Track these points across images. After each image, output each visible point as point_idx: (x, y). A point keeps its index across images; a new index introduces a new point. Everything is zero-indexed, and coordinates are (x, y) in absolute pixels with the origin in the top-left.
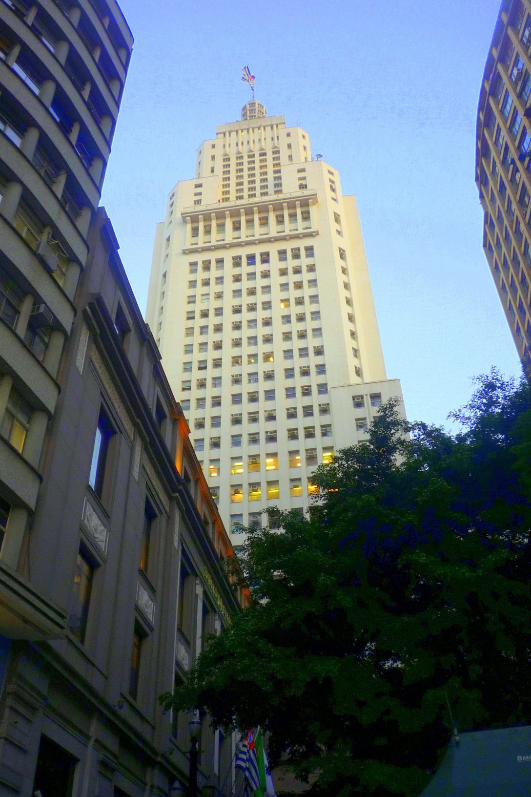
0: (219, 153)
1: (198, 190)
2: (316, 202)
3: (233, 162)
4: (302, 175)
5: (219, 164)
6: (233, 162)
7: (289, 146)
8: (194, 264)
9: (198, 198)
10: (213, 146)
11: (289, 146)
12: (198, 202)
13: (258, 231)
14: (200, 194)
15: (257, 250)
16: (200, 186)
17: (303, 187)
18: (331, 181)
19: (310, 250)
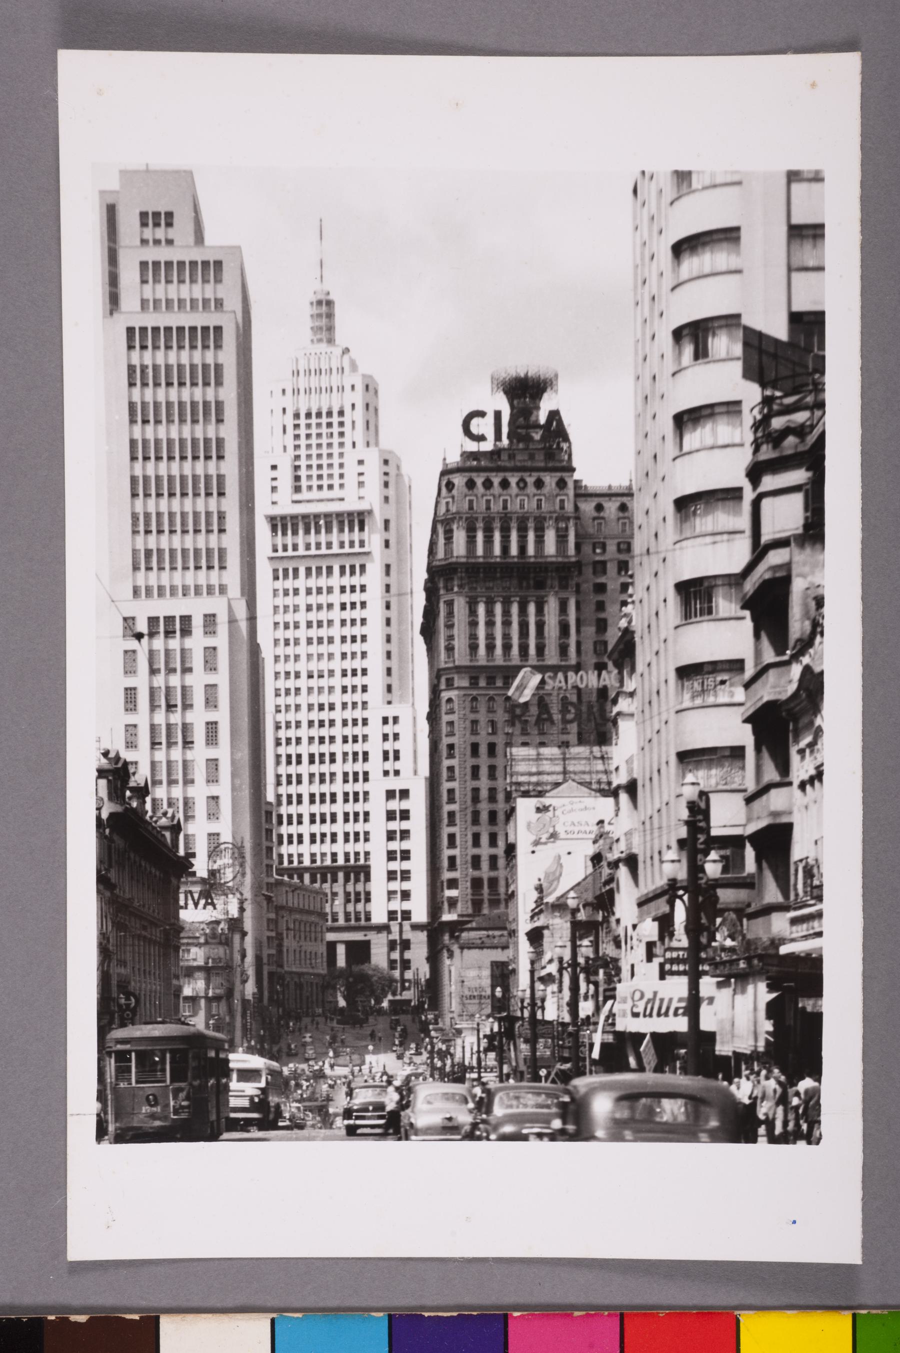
0: (288, 402)
1: (274, 474)
2: (370, 512)
3: (303, 421)
4: (361, 469)
5: (289, 421)
6: (303, 421)
7: (353, 405)
8: (275, 571)
9: (275, 483)
10: (284, 391)
11: (353, 405)
13: (323, 538)
14: (274, 479)
16: (274, 467)
17: (361, 484)
18: (386, 474)
19: (363, 568)
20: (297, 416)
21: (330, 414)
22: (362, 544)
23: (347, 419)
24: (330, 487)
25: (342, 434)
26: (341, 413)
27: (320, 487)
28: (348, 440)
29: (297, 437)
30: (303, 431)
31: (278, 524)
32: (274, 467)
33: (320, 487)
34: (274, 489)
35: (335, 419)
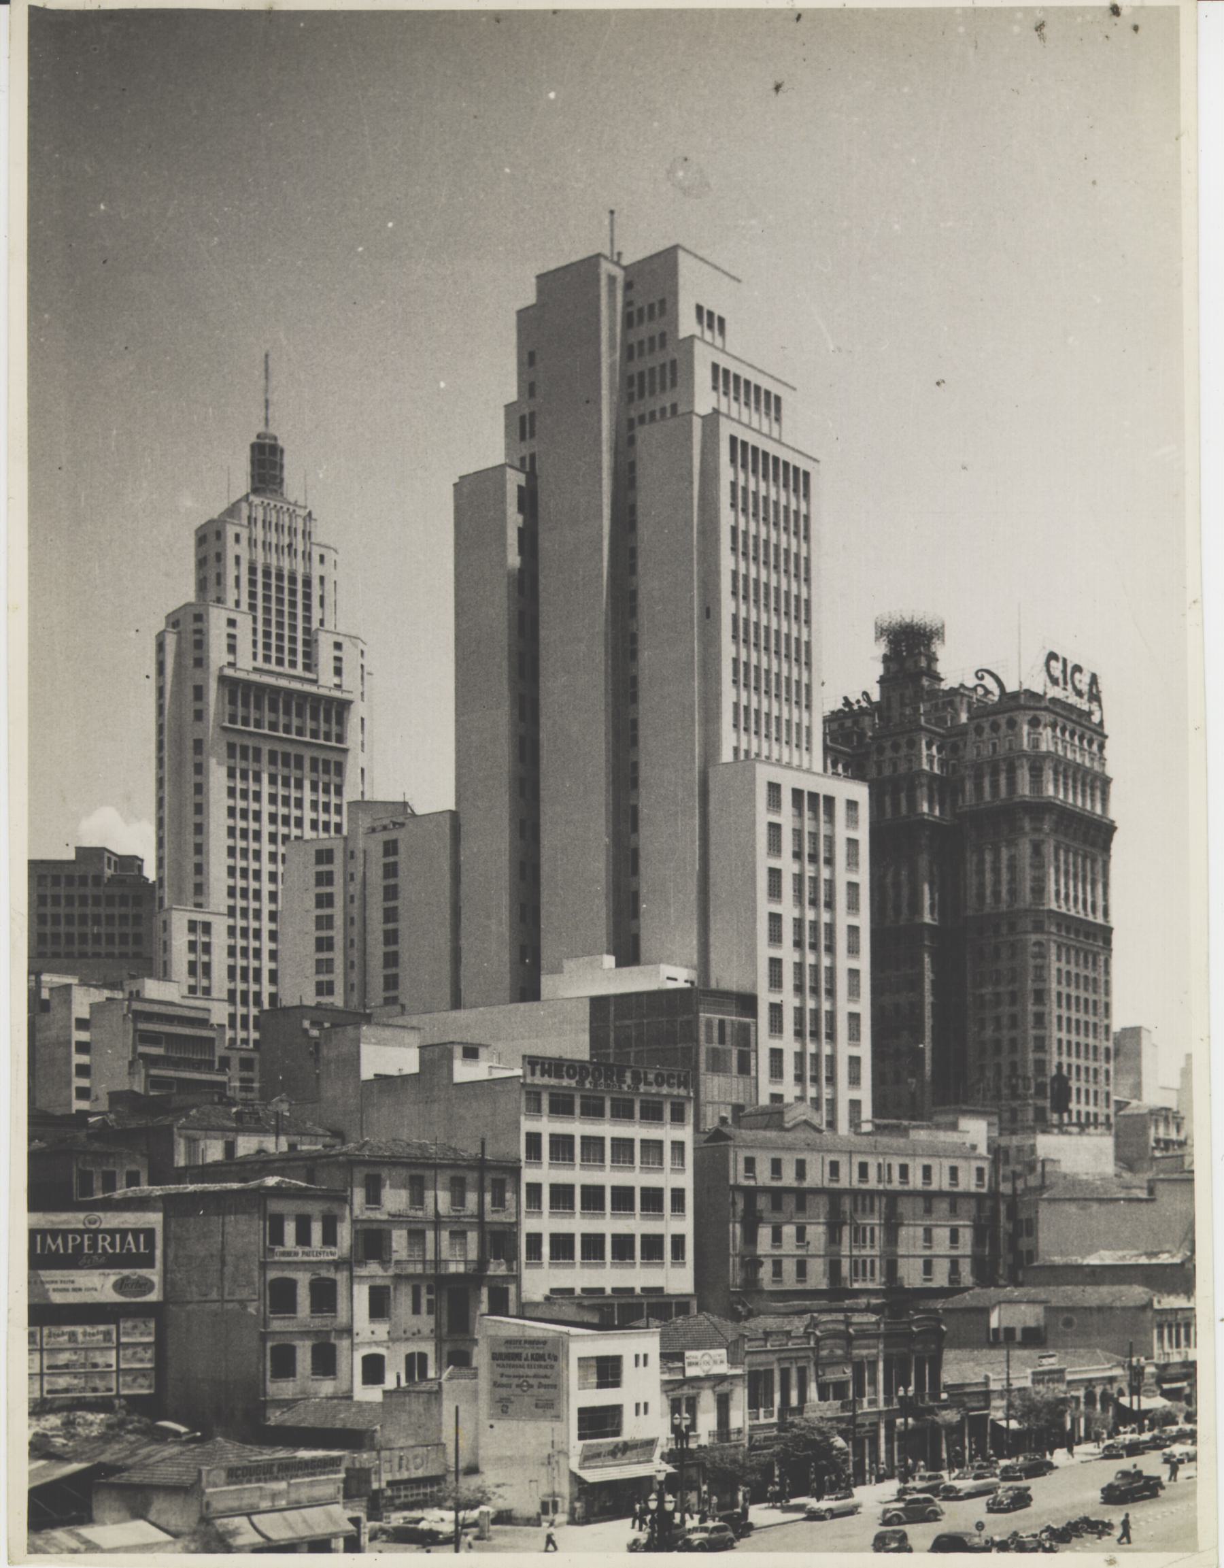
24: (293, 664)
26: (307, 583)
33: (280, 662)
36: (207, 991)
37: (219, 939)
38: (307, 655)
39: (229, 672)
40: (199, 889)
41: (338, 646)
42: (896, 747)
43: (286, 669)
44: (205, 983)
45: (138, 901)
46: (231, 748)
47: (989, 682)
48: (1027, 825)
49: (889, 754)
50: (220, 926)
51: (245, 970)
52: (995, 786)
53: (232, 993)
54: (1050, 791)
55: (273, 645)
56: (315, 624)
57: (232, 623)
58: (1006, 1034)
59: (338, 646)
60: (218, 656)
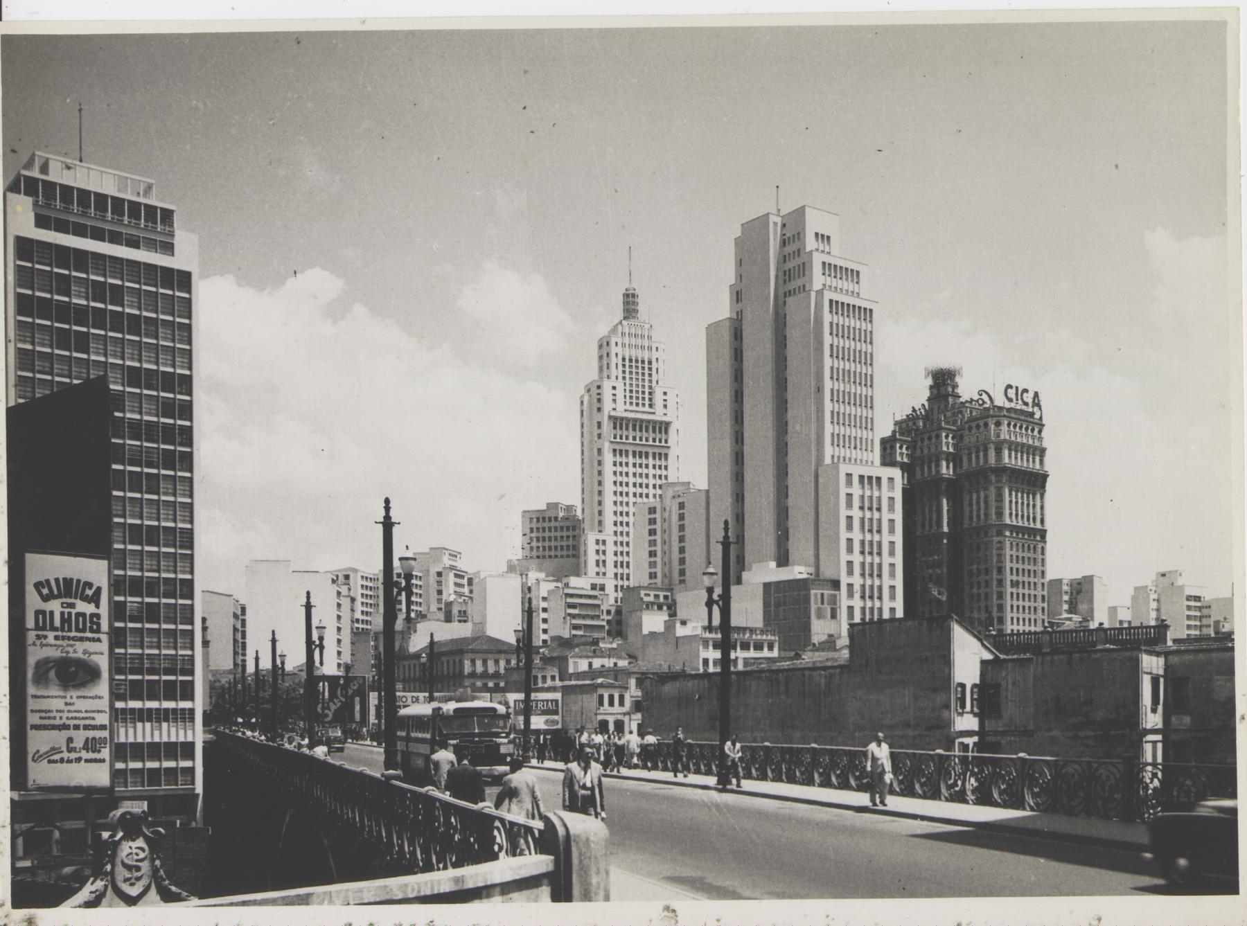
3: (627, 363)
6: (627, 363)
12: (614, 401)
15: (644, 450)
17: (665, 406)
20: (624, 359)
21: (643, 362)
22: (666, 441)
23: (654, 366)
24: (644, 405)
25: (650, 375)
26: (650, 363)
27: (637, 404)
28: (654, 378)
29: (624, 372)
30: (627, 370)
31: (617, 422)
32: (614, 388)
33: (637, 404)
34: (614, 401)
35: (646, 365)
36: (604, 574)
37: (610, 548)
38: (650, 400)
39: (613, 413)
40: (600, 523)
41: (665, 393)
42: (930, 438)
43: (640, 408)
44: (603, 570)
45: (574, 528)
46: (614, 451)
47: (985, 397)
48: (993, 478)
49: (926, 442)
50: (610, 540)
51: (622, 563)
52: (978, 458)
53: (616, 575)
54: (1006, 460)
55: (633, 396)
56: (654, 383)
57: (614, 388)
58: (982, 591)
59: (665, 393)
60: (607, 406)
